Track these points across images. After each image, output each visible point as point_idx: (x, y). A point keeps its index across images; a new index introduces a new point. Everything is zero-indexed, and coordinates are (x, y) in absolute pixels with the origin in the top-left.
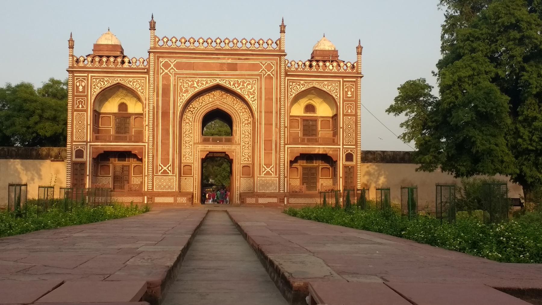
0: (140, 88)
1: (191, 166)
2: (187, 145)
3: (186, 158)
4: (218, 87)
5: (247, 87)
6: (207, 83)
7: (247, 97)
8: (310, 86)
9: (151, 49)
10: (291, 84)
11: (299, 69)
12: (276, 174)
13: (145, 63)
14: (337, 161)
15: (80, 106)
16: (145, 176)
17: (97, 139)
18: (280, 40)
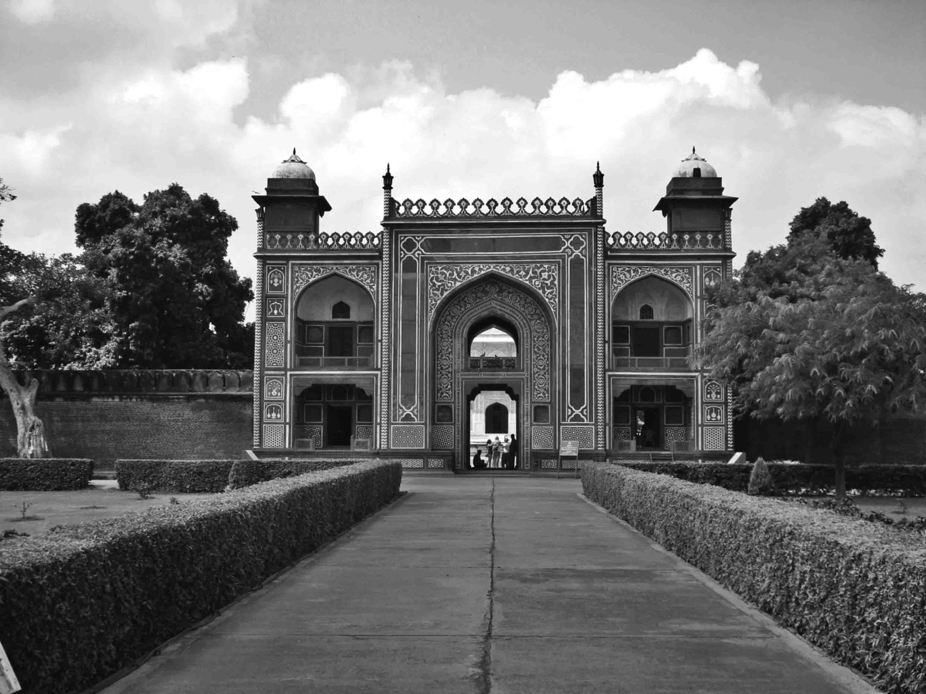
0: (368, 281)
1: (448, 408)
3: (442, 393)
4: (492, 279)
6: (473, 271)
7: (541, 292)
8: (647, 273)
9: (386, 219)
12: (591, 420)
13: (376, 241)
15: (276, 312)
16: (377, 424)
17: (303, 365)
18: (595, 198)
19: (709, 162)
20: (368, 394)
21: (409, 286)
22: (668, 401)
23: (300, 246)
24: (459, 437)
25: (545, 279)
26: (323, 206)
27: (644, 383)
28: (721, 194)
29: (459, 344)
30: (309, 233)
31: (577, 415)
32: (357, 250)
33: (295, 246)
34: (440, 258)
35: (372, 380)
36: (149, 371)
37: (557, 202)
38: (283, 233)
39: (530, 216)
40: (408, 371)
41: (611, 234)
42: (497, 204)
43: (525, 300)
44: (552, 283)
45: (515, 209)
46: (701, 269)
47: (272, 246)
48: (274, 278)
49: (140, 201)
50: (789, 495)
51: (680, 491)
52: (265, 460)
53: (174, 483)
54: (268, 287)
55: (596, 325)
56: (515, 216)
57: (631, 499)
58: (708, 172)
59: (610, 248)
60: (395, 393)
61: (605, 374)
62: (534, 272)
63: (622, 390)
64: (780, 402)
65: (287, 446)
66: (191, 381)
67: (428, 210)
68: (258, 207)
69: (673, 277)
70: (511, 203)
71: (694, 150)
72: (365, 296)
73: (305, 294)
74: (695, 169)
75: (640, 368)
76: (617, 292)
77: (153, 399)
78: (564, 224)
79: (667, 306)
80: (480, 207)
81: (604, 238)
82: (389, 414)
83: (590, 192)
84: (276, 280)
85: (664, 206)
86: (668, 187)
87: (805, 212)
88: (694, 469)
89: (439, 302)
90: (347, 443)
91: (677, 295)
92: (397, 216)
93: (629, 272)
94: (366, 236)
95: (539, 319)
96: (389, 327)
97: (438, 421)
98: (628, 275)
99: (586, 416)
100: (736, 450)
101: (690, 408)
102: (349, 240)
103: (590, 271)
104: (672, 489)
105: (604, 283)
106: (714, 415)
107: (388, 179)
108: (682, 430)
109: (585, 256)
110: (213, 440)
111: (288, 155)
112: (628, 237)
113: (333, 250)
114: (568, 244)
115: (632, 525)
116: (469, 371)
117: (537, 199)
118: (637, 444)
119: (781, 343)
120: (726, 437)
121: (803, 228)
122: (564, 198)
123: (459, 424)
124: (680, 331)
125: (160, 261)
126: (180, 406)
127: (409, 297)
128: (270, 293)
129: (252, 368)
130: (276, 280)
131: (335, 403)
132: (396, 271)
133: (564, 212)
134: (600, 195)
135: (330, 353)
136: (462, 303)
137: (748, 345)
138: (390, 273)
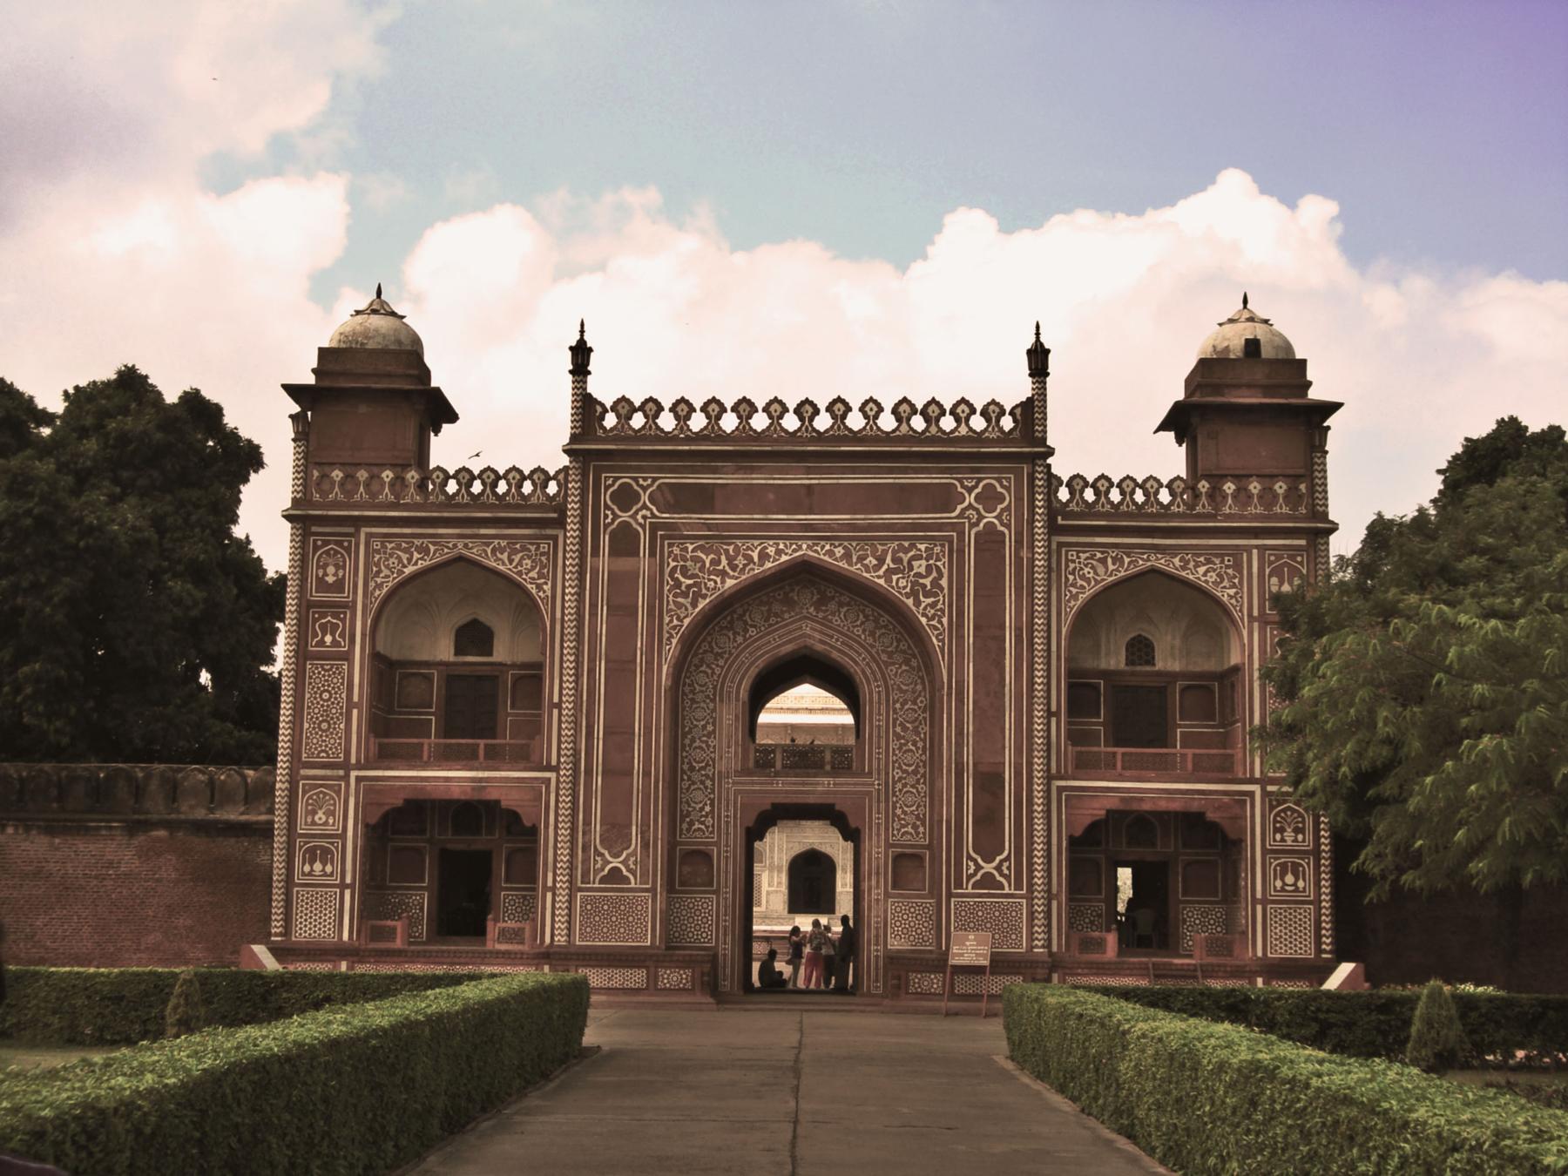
0: (534, 574)
1: (707, 857)
2: (696, 776)
3: (691, 824)
4: (804, 574)
5: (911, 568)
6: (764, 556)
7: (910, 602)
8: (1142, 565)
10: (1072, 555)
11: (1099, 508)
12: (1018, 886)
13: (552, 488)
15: (328, 639)
17: (385, 756)
19: (1278, 326)
20: (527, 823)
21: (622, 584)
23: (387, 495)
26: (439, 411)
27: (1135, 806)
29: (729, 716)
30: (406, 467)
32: (509, 507)
33: (373, 495)
34: (692, 526)
35: (536, 791)
36: (47, 766)
37: (948, 407)
38: (350, 467)
39: (887, 437)
40: (617, 772)
41: (1065, 480)
42: (816, 411)
43: (876, 621)
44: (935, 583)
45: (855, 421)
47: (324, 494)
48: (325, 566)
49: (55, 404)
50: (1486, 1066)
51: (1315, 1082)
53: (55, 1021)
54: (312, 583)
56: (855, 437)
57: (1149, 1086)
58: (1277, 348)
60: (587, 823)
61: (1049, 785)
62: (893, 561)
63: (1087, 821)
64: (1474, 851)
65: (346, 936)
66: (138, 791)
67: (667, 422)
68: (296, 409)
69: (1200, 574)
70: (849, 409)
71: (1245, 301)
72: (525, 607)
75: (1128, 773)
76: (1076, 605)
77: (50, 830)
80: (781, 417)
81: (1049, 485)
82: (572, 867)
83: (1015, 388)
84: (331, 570)
85: (1179, 421)
86: (1188, 381)
87: (1472, 446)
88: (1267, 1003)
89: (687, 621)
90: (477, 930)
91: (1206, 615)
92: (600, 433)
93: (1103, 561)
94: (530, 477)
96: (578, 676)
97: (682, 884)
98: (1101, 570)
99: (1007, 877)
100: (1341, 956)
102: (495, 485)
103: (1019, 559)
104: (1285, 1071)
106: (1290, 879)
107: (581, 353)
108: (1219, 911)
109: (1008, 526)
110: (183, 921)
112: (1102, 485)
114: (970, 499)
115: (1151, 1151)
116: (750, 774)
118: (1120, 941)
119: (1480, 707)
120: (1318, 928)
122: (963, 401)
125: (91, 530)
127: (622, 611)
128: (317, 596)
129: (272, 759)
130: (331, 570)
131: (459, 843)
132: (595, 553)
133: (963, 430)
135: (447, 731)
136: (738, 626)
138: (582, 557)
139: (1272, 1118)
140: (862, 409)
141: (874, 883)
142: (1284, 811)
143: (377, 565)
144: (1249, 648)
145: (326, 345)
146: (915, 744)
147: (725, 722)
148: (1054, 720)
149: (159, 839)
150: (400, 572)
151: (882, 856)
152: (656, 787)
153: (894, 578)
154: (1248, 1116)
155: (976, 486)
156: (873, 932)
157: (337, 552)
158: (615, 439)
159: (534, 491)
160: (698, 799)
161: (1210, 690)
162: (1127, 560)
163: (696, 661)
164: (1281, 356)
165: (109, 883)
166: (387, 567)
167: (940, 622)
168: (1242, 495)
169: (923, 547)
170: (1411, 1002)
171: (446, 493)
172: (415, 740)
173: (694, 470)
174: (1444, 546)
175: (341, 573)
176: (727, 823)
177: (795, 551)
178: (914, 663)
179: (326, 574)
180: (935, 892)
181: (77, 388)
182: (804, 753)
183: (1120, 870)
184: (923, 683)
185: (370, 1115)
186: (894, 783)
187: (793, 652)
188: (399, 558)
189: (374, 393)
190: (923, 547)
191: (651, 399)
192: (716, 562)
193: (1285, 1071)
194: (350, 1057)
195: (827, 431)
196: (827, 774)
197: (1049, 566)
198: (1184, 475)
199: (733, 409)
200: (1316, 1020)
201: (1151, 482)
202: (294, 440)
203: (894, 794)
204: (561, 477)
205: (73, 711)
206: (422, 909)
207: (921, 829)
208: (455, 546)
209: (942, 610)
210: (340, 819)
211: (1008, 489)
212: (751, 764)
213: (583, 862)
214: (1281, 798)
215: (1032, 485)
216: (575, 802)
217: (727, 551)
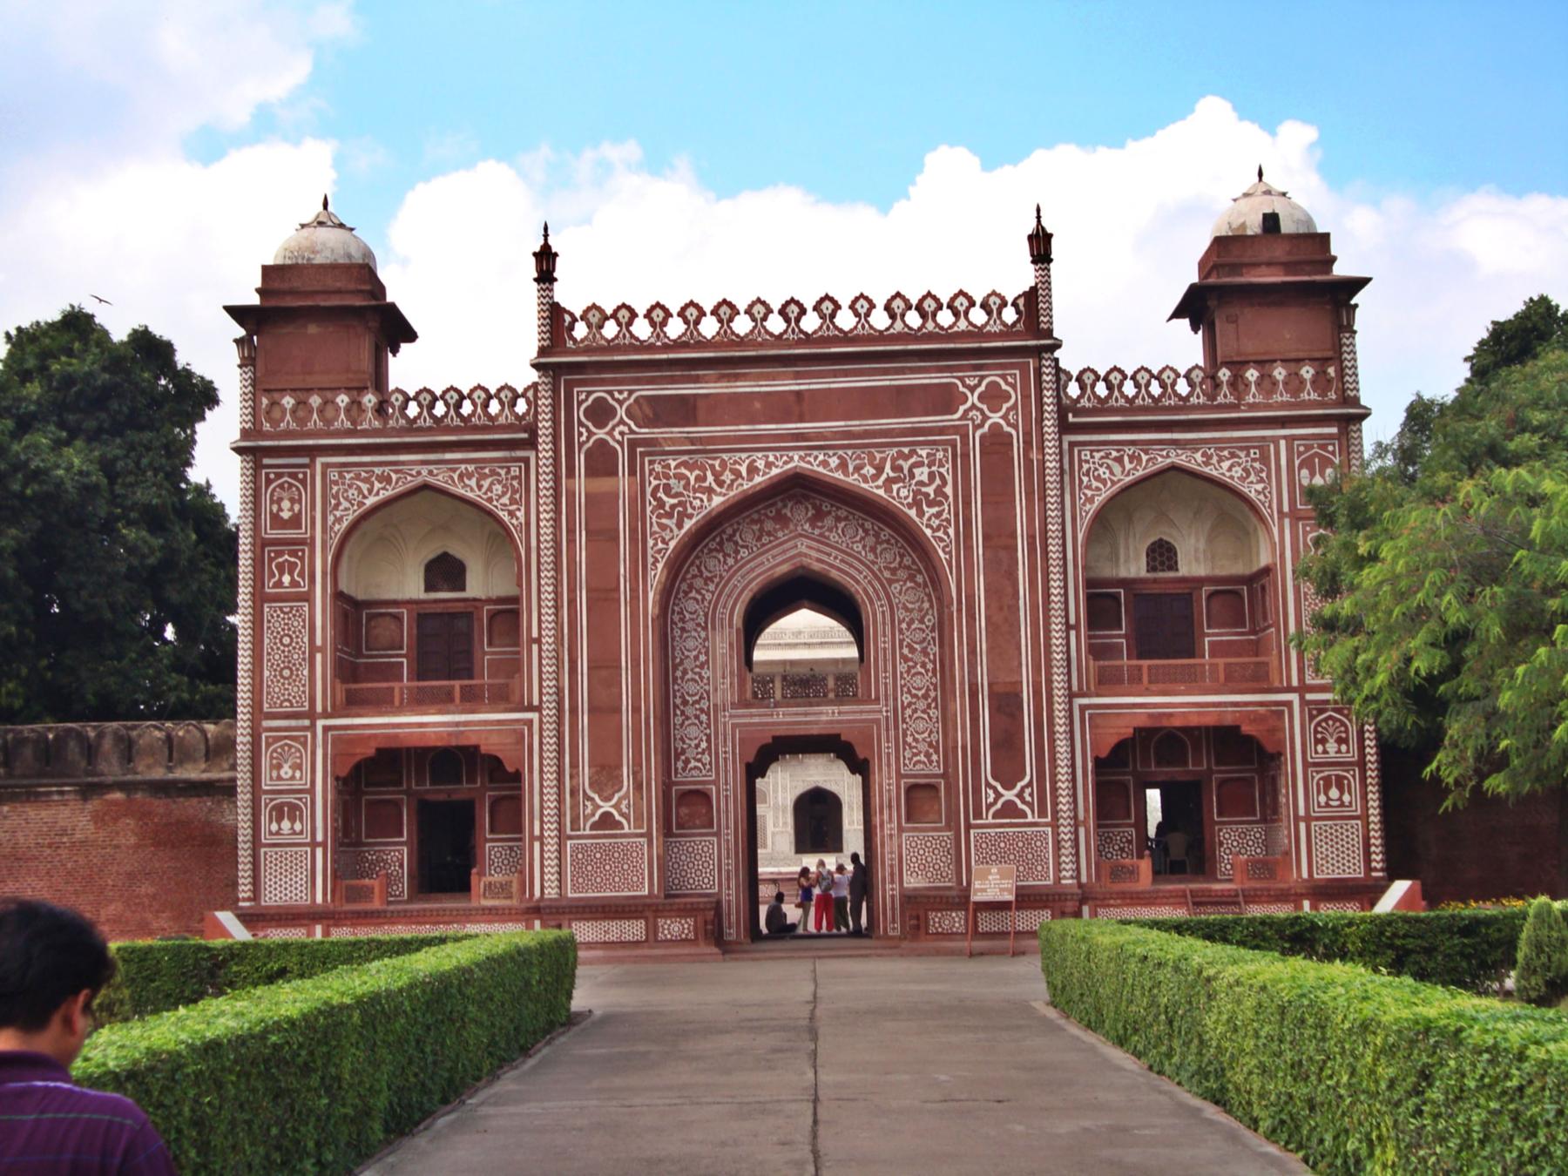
0: (505, 500)
1: (704, 796)
3: (687, 762)
4: (797, 487)
5: (912, 476)
6: (752, 470)
7: (913, 513)
8: (1161, 462)
9: (542, 351)
10: (1086, 455)
11: (1112, 402)
12: (1042, 814)
13: (521, 407)
14: (1280, 754)
15: (286, 579)
16: (532, 838)
17: (353, 703)
18: (1034, 290)
19: (1298, 198)
20: (510, 769)
21: (601, 506)
22: (1217, 764)
23: (342, 421)
24: (729, 864)
25: (921, 483)
26: (396, 330)
27: (1165, 723)
28: (1329, 270)
29: (724, 644)
30: (362, 390)
31: (1009, 803)
33: (329, 422)
34: (673, 441)
35: (519, 735)
37: (945, 300)
39: (881, 337)
40: (605, 710)
41: (1075, 374)
42: (803, 311)
43: (877, 535)
44: (939, 491)
45: (845, 320)
46: (1290, 449)
47: (275, 423)
48: (280, 500)
52: (277, 935)
54: (266, 519)
55: (1047, 588)
56: (846, 337)
57: (1249, 1044)
58: (1298, 222)
59: (1074, 407)
61: (1070, 703)
62: (894, 469)
63: (1113, 741)
65: (319, 899)
66: (91, 751)
67: (642, 329)
68: (241, 332)
69: (1222, 470)
70: (837, 307)
71: (1260, 174)
72: (499, 536)
73: (353, 539)
74: (1265, 216)
75: (1153, 687)
76: (1091, 509)
78: (968, 351)
79: (1210, 540)
80: (765, 318)
81: (1058, 380)
82: (560, 815)
83: (1018, 277)
84: (286, 504)
85: (1194, 307)
86: (1202, 264)
87: (1500, 332)
88: (1334, 929)
89: (672, 544)
90: (463, 887)
91: (1230, 509)
92: (570, 344)
93: (1119, 460)
94: (497, 395)
95: (912, 578)
96: (557, 608)
97: (680, 826)
99: (1030, 805)
100: (1393, 874)
101: (1274, 780)
102: (458, 405)
103: (1028, 462)
105: (1062, 489)
106: (1334, 793)
107: (546, 259)
108: (1257, 831)
109: (1015, 427)
110: (146, 889)
111: (313, 210)
112: (1115, 378)
113: (421, 430)
114: (973, 399)
115: (1254, 1124)
116: (748, 705)
117: (898, 295)
120: (1367, 845)
121: (1497, 365)
123: (729, 834)
124: (1245, 597)
125: (37, 475)
126: (64, 813)
127: (602, 536)
130: (286, 504)
133: (962, 325)
134: (1045, 280)
135: (420, 673)
136: (729, 547)
137: (1468, 598)
139: (1458, 1099)
140: (852, 307)
141: (886, 817)
142: (1326, 720)
143: (336, 497)
144: (1281, 547)
145: (270, 262)
146: (924, 665)
147: (719, 651)
148: (1073, 633)
149: (116, 803)
150: (361, 504)
151: (894, 788)
152: (647, 724)
153: (895, 487)
154: (1416, 1091)
155: (977, 386)
156: (888, 870)
157: (291, 485)
158: (588, 350)
159: (502, 410)
160: (692, 734)
161: (1238, 594)
162: (1145, 458)
163: (684, 587)
164: (1302, 230)
165: (64, 852)
166: (346, 499)
167: (946, 533)
168: (1267, 383)
169: (924, 453)
170: (1512, 924)
171: (405, 417)
172: (385, 685)
173: (673, 380)
174: (1491, 426)
175: (296, 507)
176: (725, 759)
177: (786, 463)
178: (919, 579)
179: (280, 509)
180: (952, 824)
181: (19, 329)
182: (805, 682)
183: (1149, 792)
184: (930, 601)
185: (274, 1131)
186: (904, 709)
187: (790, 572)
188: (359, 489)
189: (325, 313)
190: (924, 453)
191: (624, 306)
192: (703, 479)
193: (1474, 1035)
194: (236, 1062)
195: (815, 332)
196: (831, 703)
197: (1061, 468)
198: (1201, 364)
199: (712, 313)
200: (1391, 946)
201: (1168, 372)
202: (240, 366)
203: (904, 721)
204: (530, 394)
205: (24, 671)
206: (401, 866)
207: (935, 757)
208: (419, 473)
209: (948, 521)
210: (305, 773)
211: (1014, 386)
212: (749, 695)
213: (572, 808)
214: (1321, 707)
215: (1039, 381)
216: (560, 744)
217: (712, 467)
